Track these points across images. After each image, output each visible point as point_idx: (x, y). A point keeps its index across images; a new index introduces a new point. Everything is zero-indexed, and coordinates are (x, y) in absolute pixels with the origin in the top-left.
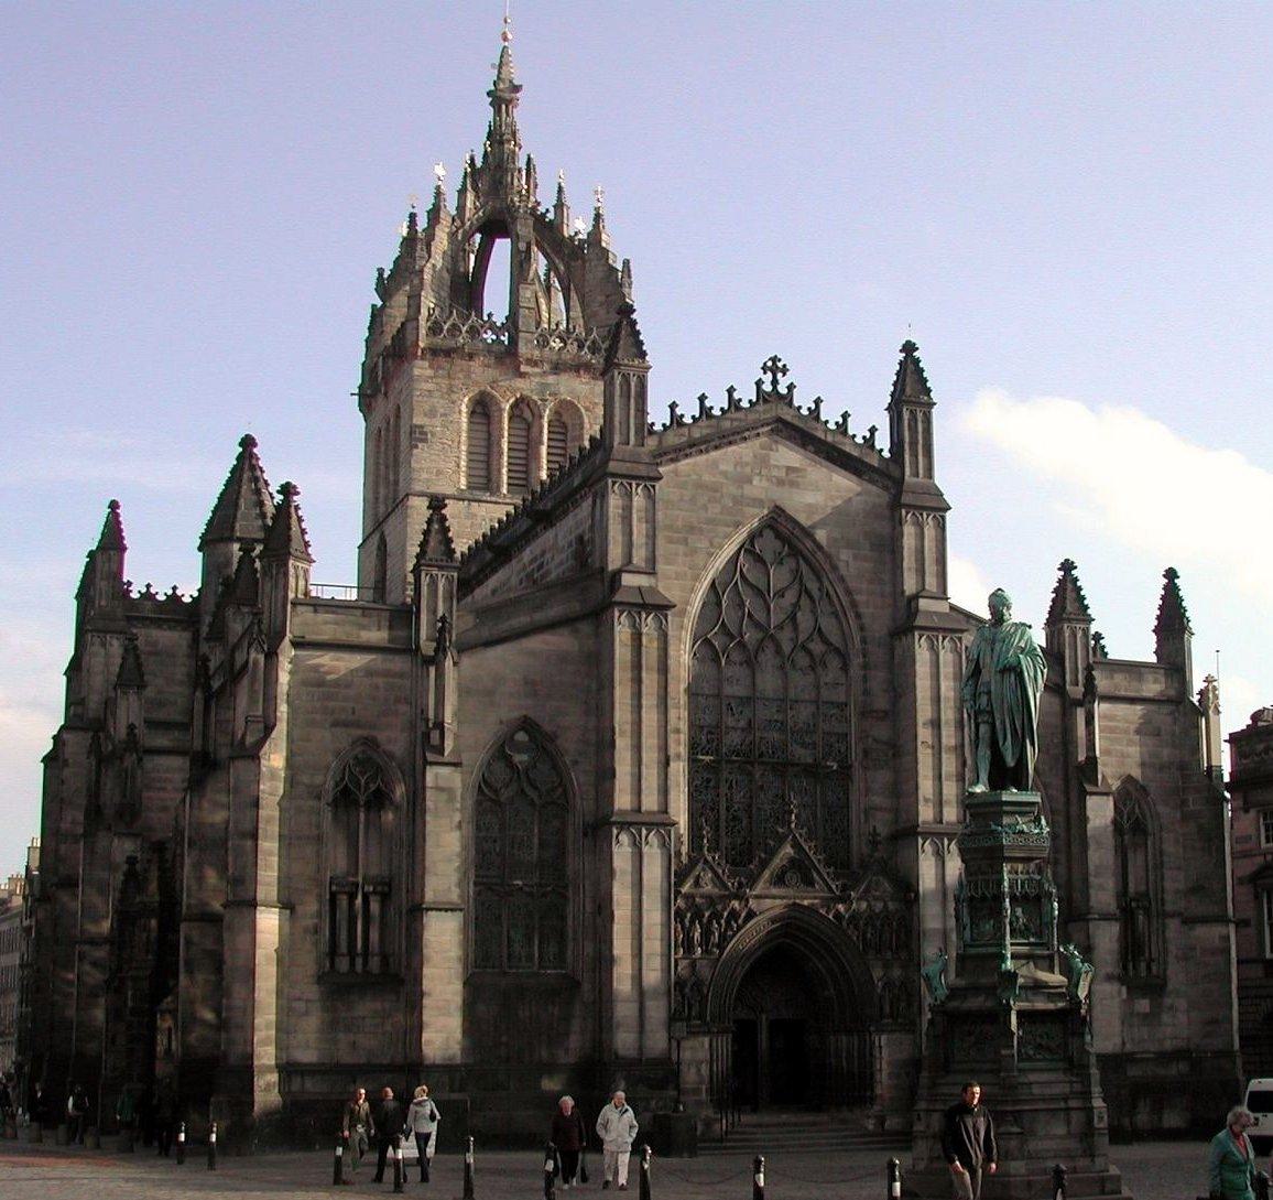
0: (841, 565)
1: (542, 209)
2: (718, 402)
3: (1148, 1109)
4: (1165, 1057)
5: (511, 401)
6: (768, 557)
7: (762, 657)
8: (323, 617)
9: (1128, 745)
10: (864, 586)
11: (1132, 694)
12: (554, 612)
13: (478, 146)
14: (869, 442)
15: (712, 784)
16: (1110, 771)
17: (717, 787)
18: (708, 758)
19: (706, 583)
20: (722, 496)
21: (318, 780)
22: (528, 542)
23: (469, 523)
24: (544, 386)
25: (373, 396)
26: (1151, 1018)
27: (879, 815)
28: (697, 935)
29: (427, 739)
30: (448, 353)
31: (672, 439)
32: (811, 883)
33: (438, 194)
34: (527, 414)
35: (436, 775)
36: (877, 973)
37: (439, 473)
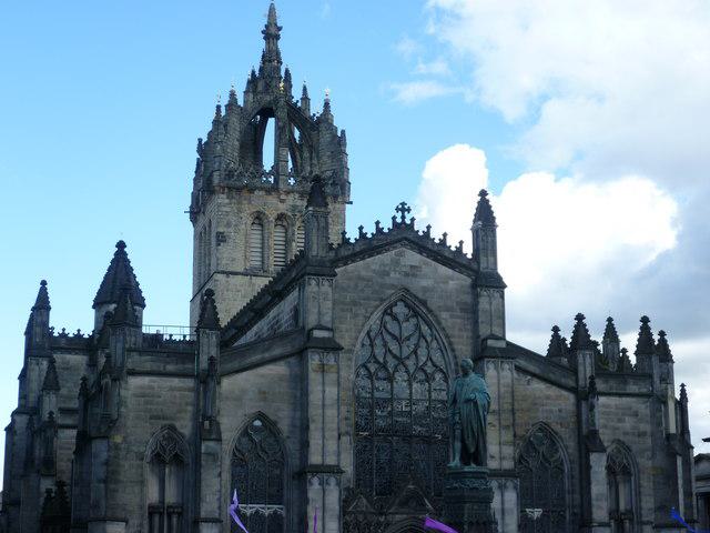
0: (443, 321)
1: (294, 100)
2: (370, 230)
5: (275, 215)
6: (401, 318)
7: (397, 375)
8: (144, 358)
10: (456, 333)
12: (277, 351)
13: (256, 63)
14: (459, 250)
16: (605, 436)
17: (371, 450)
19: (363, 334)
21: (142, 449)
22: (272, 307)
23: (250, 289)
24: (294, 207)
25: (198, 213)
29: (207, 424)
30: (239, 190)
31: (344, 252)
32: (424, 505)
33: (232, 95)
34: (285, 224)
35: (207, 447)
37: (233, 260)
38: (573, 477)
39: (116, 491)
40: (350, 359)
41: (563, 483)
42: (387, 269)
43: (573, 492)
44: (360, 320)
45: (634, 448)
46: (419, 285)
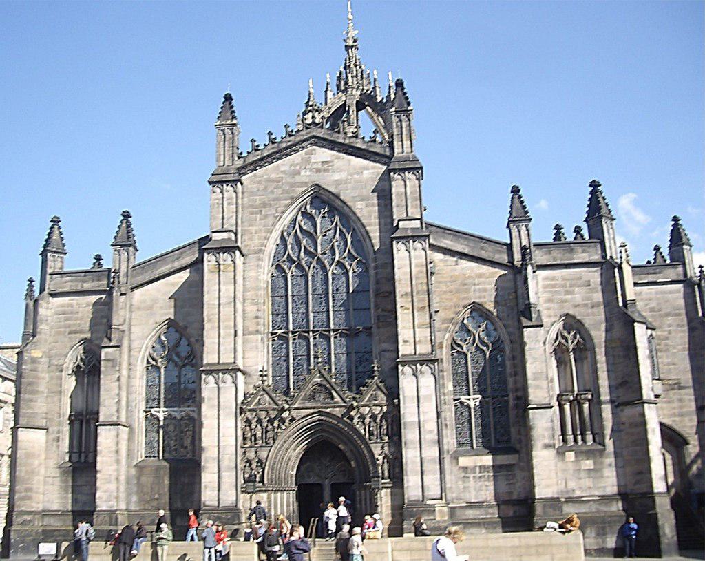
0: (357, 212)
2: (279, 134)
3: (593, 535)
4: (605, 499)
9: (565, 295)
11: (567, 262)
15: (284, 346)
18: (280, 332)
19: (276, 235)
20: (283, 184)
21: (61, 362)
26: (595, 472)
27: (387, 354)
28: (259, 434)
31: (251, 159)
32: (333, 398)
35: (106, 353)
36: (377, 450)
38: (514, 358)
39: (31, 401)
40: (262, 260)
41: (503, 365)
42: (298, 167)
43: (516, 374)
44: (270, 221)
45: (587, 322)
46: (329, 181)
